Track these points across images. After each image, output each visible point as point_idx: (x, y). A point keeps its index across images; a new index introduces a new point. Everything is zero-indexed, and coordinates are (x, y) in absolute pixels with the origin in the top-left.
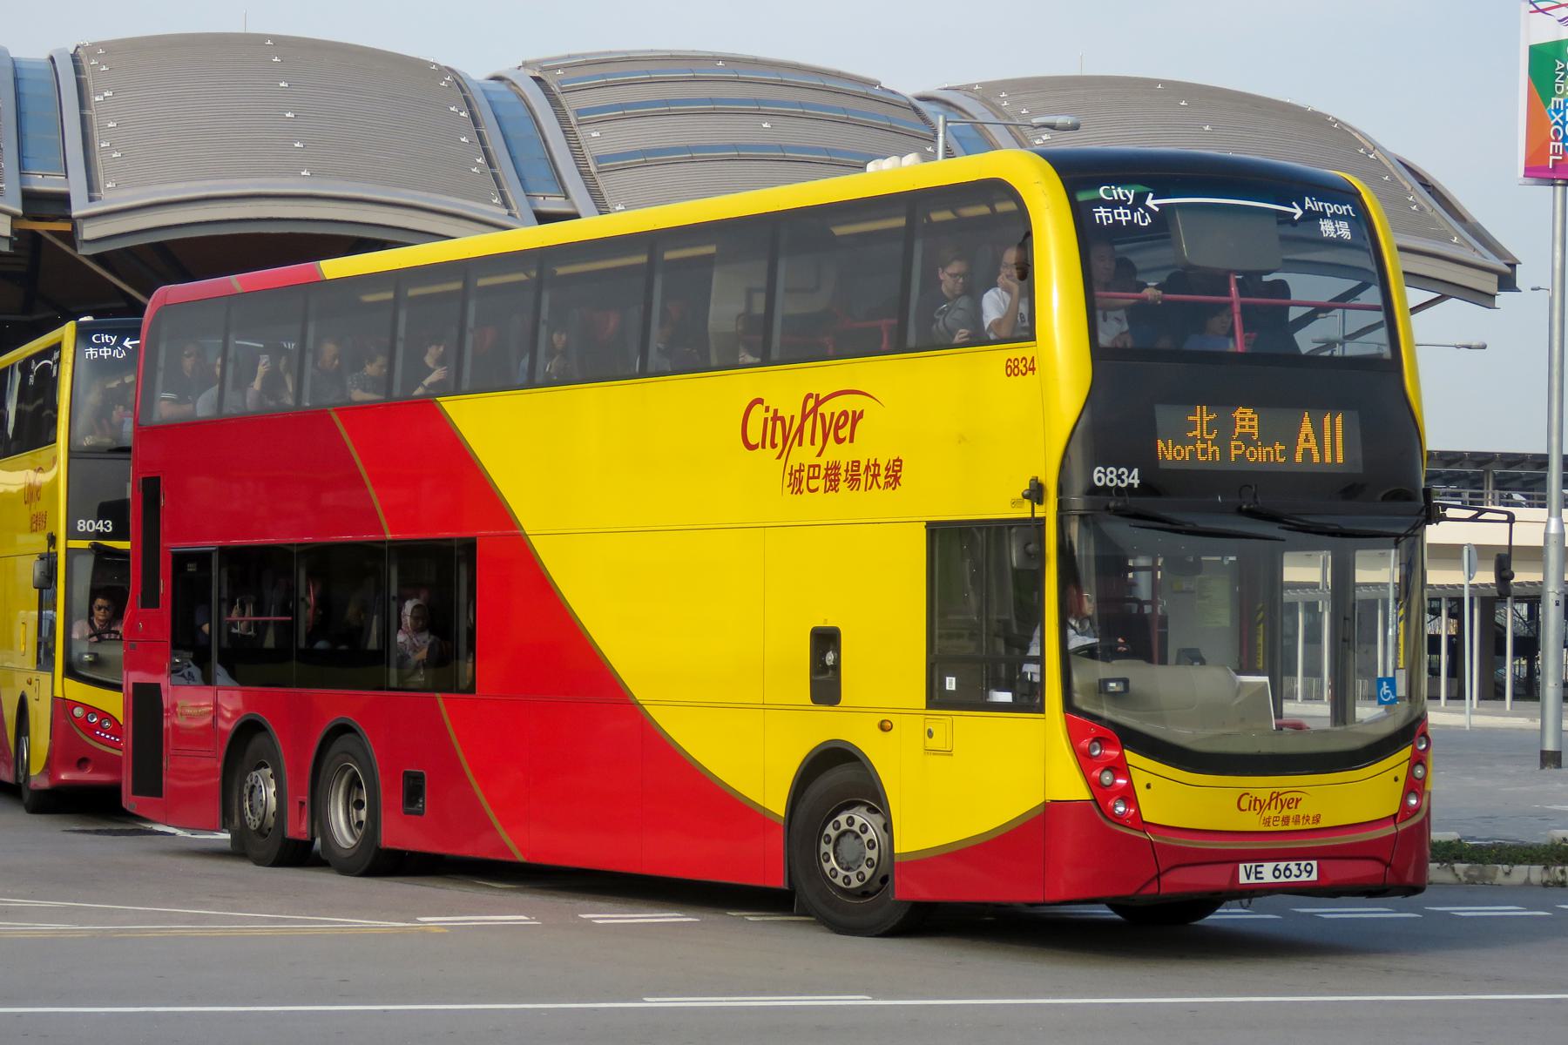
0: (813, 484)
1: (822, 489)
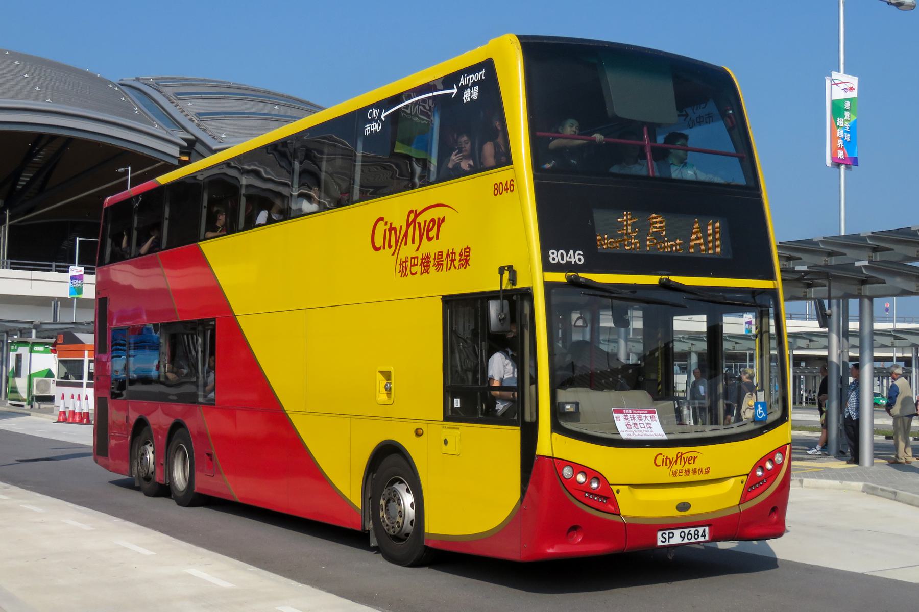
0: (414, 269)
1: (419, 273)
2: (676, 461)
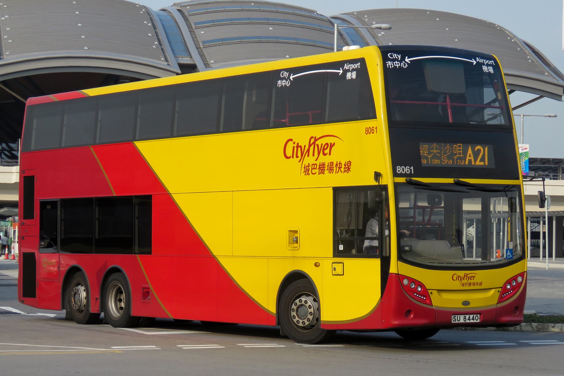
0: (314, 171)
1: (317, 173)
2: (464, 278)
